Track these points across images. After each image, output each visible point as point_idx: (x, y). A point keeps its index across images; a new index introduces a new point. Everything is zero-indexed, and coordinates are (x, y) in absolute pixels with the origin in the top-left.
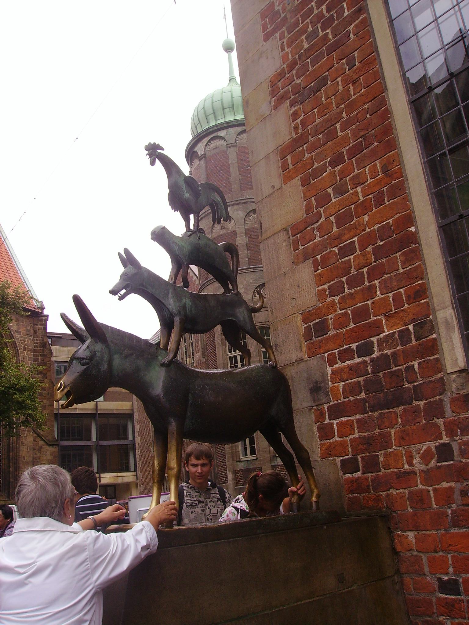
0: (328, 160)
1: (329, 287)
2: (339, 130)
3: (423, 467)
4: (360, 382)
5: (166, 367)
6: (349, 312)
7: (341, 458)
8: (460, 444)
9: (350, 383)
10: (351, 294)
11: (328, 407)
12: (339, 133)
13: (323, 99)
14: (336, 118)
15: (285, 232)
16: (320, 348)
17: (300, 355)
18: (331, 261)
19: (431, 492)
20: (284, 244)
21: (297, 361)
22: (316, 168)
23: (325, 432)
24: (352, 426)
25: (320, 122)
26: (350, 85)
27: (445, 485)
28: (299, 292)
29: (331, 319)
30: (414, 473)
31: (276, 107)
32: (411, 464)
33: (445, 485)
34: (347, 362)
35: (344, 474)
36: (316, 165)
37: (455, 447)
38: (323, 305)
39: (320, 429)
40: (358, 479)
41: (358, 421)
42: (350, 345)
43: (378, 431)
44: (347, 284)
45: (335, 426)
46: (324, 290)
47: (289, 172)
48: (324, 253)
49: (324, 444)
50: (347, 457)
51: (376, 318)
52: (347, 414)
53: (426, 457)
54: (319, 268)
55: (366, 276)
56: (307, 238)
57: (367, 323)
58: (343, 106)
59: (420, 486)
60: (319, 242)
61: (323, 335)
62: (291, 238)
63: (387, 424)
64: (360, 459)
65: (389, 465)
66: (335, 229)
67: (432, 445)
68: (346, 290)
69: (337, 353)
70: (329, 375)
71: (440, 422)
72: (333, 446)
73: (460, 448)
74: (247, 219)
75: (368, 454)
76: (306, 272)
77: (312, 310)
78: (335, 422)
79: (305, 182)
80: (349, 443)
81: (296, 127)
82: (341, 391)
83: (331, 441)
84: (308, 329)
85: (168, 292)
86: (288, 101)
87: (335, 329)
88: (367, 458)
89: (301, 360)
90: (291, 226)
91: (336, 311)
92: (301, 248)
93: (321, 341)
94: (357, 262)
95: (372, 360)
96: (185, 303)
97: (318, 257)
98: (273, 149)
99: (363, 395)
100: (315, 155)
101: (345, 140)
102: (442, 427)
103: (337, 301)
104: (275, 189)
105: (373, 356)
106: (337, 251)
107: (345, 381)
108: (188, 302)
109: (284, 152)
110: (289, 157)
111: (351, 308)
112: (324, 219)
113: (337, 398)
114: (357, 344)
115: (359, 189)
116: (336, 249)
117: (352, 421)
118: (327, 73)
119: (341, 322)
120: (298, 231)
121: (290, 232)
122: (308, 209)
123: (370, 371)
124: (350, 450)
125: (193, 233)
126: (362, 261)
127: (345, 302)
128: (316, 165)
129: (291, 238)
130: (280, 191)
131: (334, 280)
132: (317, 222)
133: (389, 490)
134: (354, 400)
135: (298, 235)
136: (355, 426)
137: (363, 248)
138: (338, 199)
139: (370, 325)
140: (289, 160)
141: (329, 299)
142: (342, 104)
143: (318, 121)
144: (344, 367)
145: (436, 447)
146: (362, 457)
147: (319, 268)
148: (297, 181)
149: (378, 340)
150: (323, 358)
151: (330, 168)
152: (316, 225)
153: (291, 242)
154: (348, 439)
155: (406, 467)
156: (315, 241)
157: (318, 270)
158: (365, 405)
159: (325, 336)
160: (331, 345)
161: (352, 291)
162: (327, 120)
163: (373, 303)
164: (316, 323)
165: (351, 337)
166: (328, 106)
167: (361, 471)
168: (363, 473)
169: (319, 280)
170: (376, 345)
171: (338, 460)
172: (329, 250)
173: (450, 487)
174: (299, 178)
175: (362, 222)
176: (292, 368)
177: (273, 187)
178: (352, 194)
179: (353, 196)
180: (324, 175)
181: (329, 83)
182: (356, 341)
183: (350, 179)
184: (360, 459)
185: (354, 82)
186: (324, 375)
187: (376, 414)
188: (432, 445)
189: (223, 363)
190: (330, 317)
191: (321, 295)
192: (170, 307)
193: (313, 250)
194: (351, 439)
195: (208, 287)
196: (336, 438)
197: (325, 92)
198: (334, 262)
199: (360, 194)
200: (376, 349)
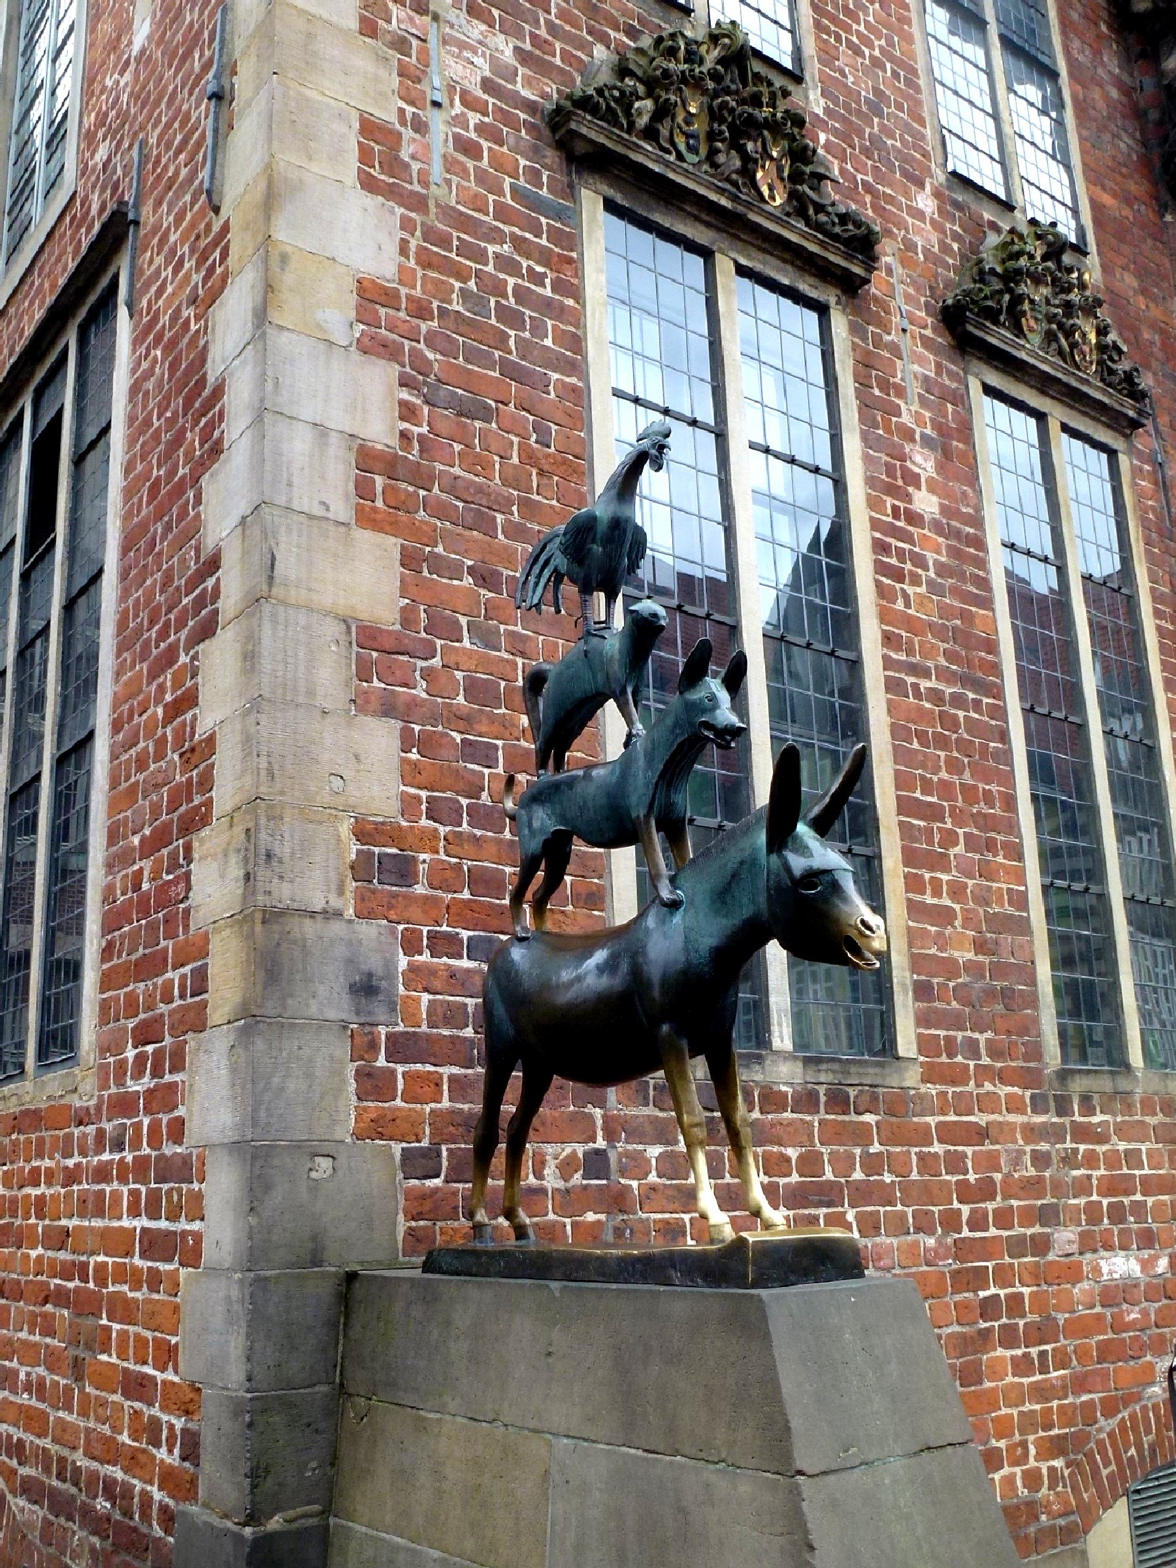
0: (470, 563)
3: (560, 1184)
7: (405, 1145)
8: (620, 1155)
9: (448, 1002)
11: (389, 1036)
12: (501, 536)
16: (391, 907)
17: (335, 902)
19: (569, 1228)
21: (325, 912)
23: (373, 1085)
24: (438, 1085)
27: (590, 1217)
30: (542, 1191)
32: (539, 1175)
33: (590, 1217)
34: (445, 959)
37: (613, 1156)
39: (359, 1074)
40: (437, 1190)
41: (452, 1079)
45: (400, 1077)
46: (418, 799)
48: (429, 728)
49: (365, 1109)
52: (432, 1060)
53: (566, 1167)
54: (414, 750)
59: (551, 1216)
64: (445, 1154)
66: (461, 699)
67: (580, 1149)
71: (598, 1112)
72: (389, 1117)
73: (620, 1161)
76: (381, 739)
77: (383, 823)
78: (400, 1069)
83: (386, 1105)
89: (338, 914)
91: (437, 852)
93: (395, 896)
97: (417, 728)
102: (599, 1123)
104: (330, 515)
113: (411, 1017)
114: (471, 933)
118: (493, 404)
119: (442, 878)
122: (407, 618)
127: (462, 846)
130: (342, 529)
132: (426, 659)
135: (375, 654)
143: (456, 471)
145: (585, 1154)
147: (414, 750)
150: (393, 932)
152: (421, 664)
153: (354, 656)
155: (532, 1180)
161: (478, 833)
162: (480, 490)
165: (462, 914)
167: (442, 1177)
168: (447, 1181)
169: (410, 772)
171: (397, 1148)
173: (599, 1221)
176: (308, 922)
178: (507, 661)
180: (455, 582)
184: (445, 1154)
185: (541, 473)
186: (390, 964)
188: (580, 1149)
190: (422, 856)
194: (432, 1111)
196: (399, 1102)
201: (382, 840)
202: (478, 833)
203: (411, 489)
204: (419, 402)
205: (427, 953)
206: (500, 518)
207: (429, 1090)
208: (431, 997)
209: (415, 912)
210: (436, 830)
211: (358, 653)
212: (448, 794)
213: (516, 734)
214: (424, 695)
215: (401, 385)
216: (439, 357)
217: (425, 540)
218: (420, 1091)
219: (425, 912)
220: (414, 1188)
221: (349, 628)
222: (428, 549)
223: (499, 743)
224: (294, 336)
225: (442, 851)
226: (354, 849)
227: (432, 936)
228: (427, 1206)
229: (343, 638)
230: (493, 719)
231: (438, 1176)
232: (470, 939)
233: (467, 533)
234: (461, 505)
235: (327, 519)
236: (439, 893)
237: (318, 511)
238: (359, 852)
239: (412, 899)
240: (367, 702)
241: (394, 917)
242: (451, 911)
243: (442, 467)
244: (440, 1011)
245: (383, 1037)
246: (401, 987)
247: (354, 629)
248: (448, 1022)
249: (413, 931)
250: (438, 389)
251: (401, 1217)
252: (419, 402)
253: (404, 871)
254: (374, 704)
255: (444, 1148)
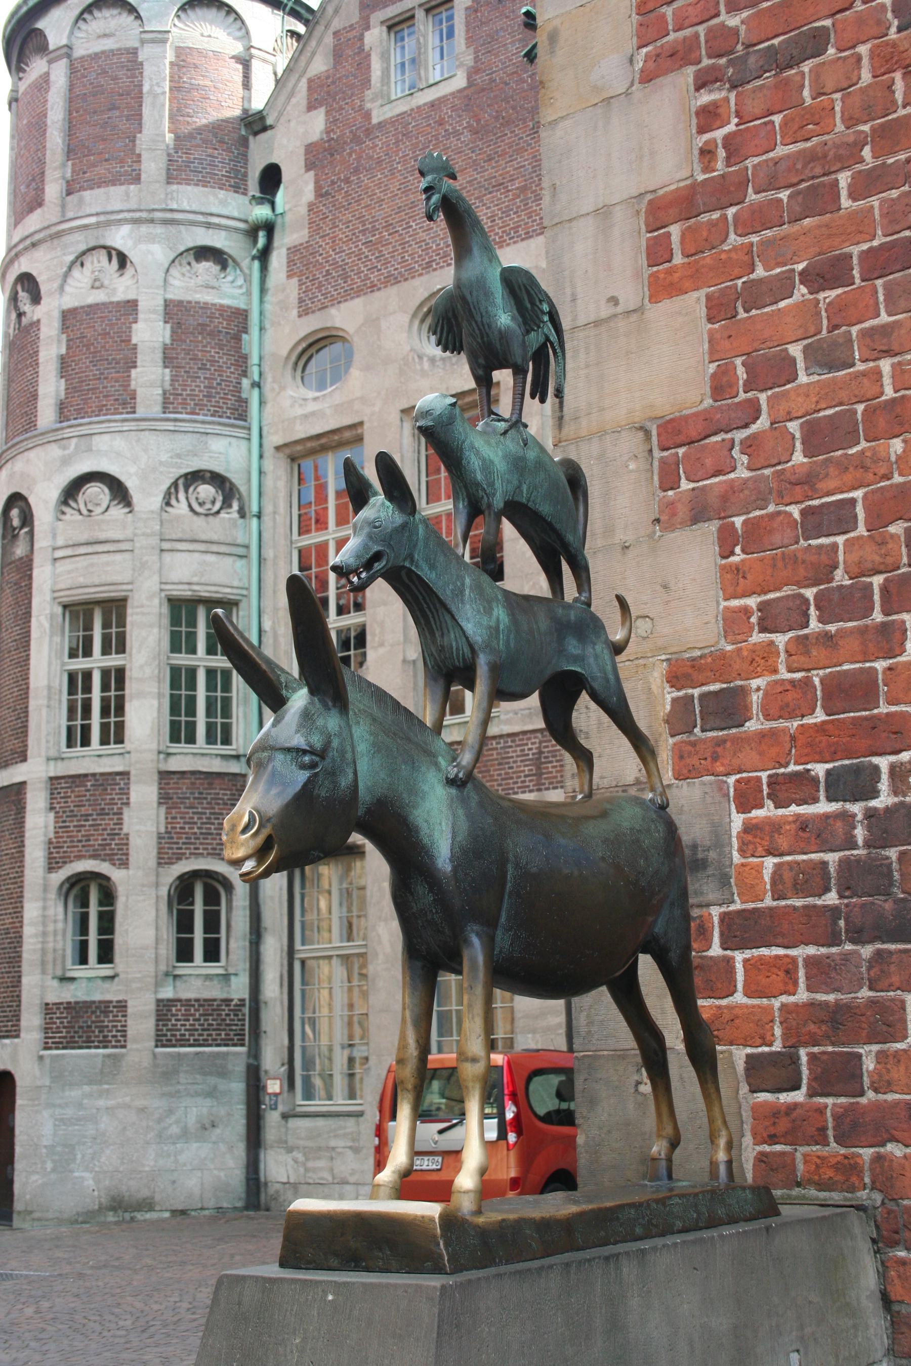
0: (800, 267)
1: (762, 607)
2: (844, 193)
4: (825, 864)
5: (458, 786)
6: (817, 681)
7: (749, 1050)
9: (798, 863)
10: (828, 636)
11: (723, 917)
12: (845, 202)
13: (806, 93)
14: (839, 158)
15: (641, 434)
16: (715, 758)
18: (777, 539)
20: (632, 466)
22: (761, 281)
25: (788, 156)
26: (898, 76)
28: (667, 603)
29: (758, 689)
31: (647, 77)
34: (794, 809)
35: (753, 1091)
36: (760, 272)
38: (739, 650)
40: (793, 1107)
41: (810, 962)
42: (809, 767)
43: (865, 993)
44: (818, 607)
46: (746, 611)
47: (669, 272)
48: (758, 513)
50: (766, 1049)
51: (893, 709)
52: (780, 940)
54: (738, 549)
55: (877, 597)
56: (708, 462)
57: (865, 718)
58: (866, 128)
60: (746, 481)
61: (730, 728)
62: (657, 454)
63: (895, 979)
64: (804, 1059)
65: (889, 1083)
66: (799, 457)
68: (814, 625)
69: (765, 781)
70: (734, 833)
72: (727, 1016)
74: (174, 272)
75: (830, 1049)
77: (701, 657)
78: (739, 957)
79: (718, 309)
80: (777, 1014)
81: (709, 152)
82: (767, 878)
83: (724, 1002)
84: (683, 705)
85: (463, 584)
86: (690, 70)
87: (768, 717)
88: (825, 1057)
90: (660, 422)
91: (775, 671)
92: (685, 485)
93: (720, 742)
94: (854, 557)
95: (870, 814)
96: (498, 619)
98: (625, 197)
99: (831, 898)
100: (761, 243)
101: (861, 225)
103: (781, 648)
104: (619, 309)
105: (874, 803)
106: (797, 515)
107: (781, 855)
108: (500, 613)
109: (660, 211)
110: (675, 231)
111: (821, 672)
112: (768, 424)
113: (751, 891)
115: (886, 365)
116: (795, 511)
117: (794, 960)
118: (828, 23)
119: (785, 701)
120: (681, 438)
121: (655, 439)
122: (721, 386)
123: (860, 842)
124: (778, 1031)
125: (511, 427)
126: (872, 556)
127: (807, 653)
128: (760, 272)
129: (657, 454)
130: (634, 317)
131: (778, 589)
132: (746, 426)
133: (883, 1145)
134: (805, 907)
135: (681, 451)
136: (801, 973)
137: (877, 522)
138: (816, 378)
139: (874, 724)
140: (675, 238)
141: (757, 637)
142: (865, 122)
143: (781, 151)
144: (784, 820)
146: (812, 1057)
147: (738, 549)
148: (695, 302)
149: (893, 768)
150: (721, 788)
151: (804, 290)
152: (739, 435)
153: (656, 464)
154: (776, 1003)
156: (732, 476)
157: (732, 553)
158: (835, 924)
159: (734, 731)
160: (749, 756)
161: (832, 628)
162: (811, 157)
163: (890, 669)
164: (710, 693)
165: (814, 744)
166: (819, 117)
167: (804, 1089)
169: (734, 581)
170: (885, 777)
172: (771, 508)
174: (702, 293)
175: (883, 454)
177: (614, 300)
178: (864, 374)
179: (865, 381)
180: (782, 304)
181: (831, 51)
182: (828, 758)
183: (863, 333)
184: (804, 1059)
187: (867, 951)
189: (49, 688)
190: (755, 683)
191: (734, 623)
192: (469, 627)
193: (724, 498)
195: (32, 454)
196: (739, 998)
197: (816, 72)
198: (786, 541)
199: (887, 381)
200: (884, 785)
201: (701, 678)
202: (832, 628)
203: (716, 215)
204: (724, 94)
205: (769, 803)
206: (844, 179)
207: (778, 978)
208: (776, 860)
209: (749, 756)
210: (772, 643)
211: (662, 461)
212: (787, 591)
213: (882, 471)
214: (746, 474)
215: (697, 89)
216: (745, 14)
217: (737, 271)
218: (764, 981)
219: (761, 754)
220: (766, 1103)
221: (647, 434)
222: (739, 282)
223: (858, 494)
224: (568, 123)
225: (782, 668)
226: (669, 698)
227: (773, 781)
228: (783, 1125)
229: (641, 449)
230: (843, 466)
231: (798, 1088)
232: (828, 773)
233: (796, 227)
234: (784, 195)
235: (615, 316)
236: (781, 724)
237: (605, 311)
238: (674, 701)
239: (739, 741)
240: (674, 514)
241: (721, 769)
242: (799, 743)
243: (756, 160)
244: (787, 875)
245: (716, 920)
246: (735, 854)
247: (654, 433)
248: (800, 889)
249: (748, 780)
250: (744, 59)
251: (748, 1140)
252: (724, 94)
253: (728, 708)
254: (683, 511)
255: (803, 1053)
